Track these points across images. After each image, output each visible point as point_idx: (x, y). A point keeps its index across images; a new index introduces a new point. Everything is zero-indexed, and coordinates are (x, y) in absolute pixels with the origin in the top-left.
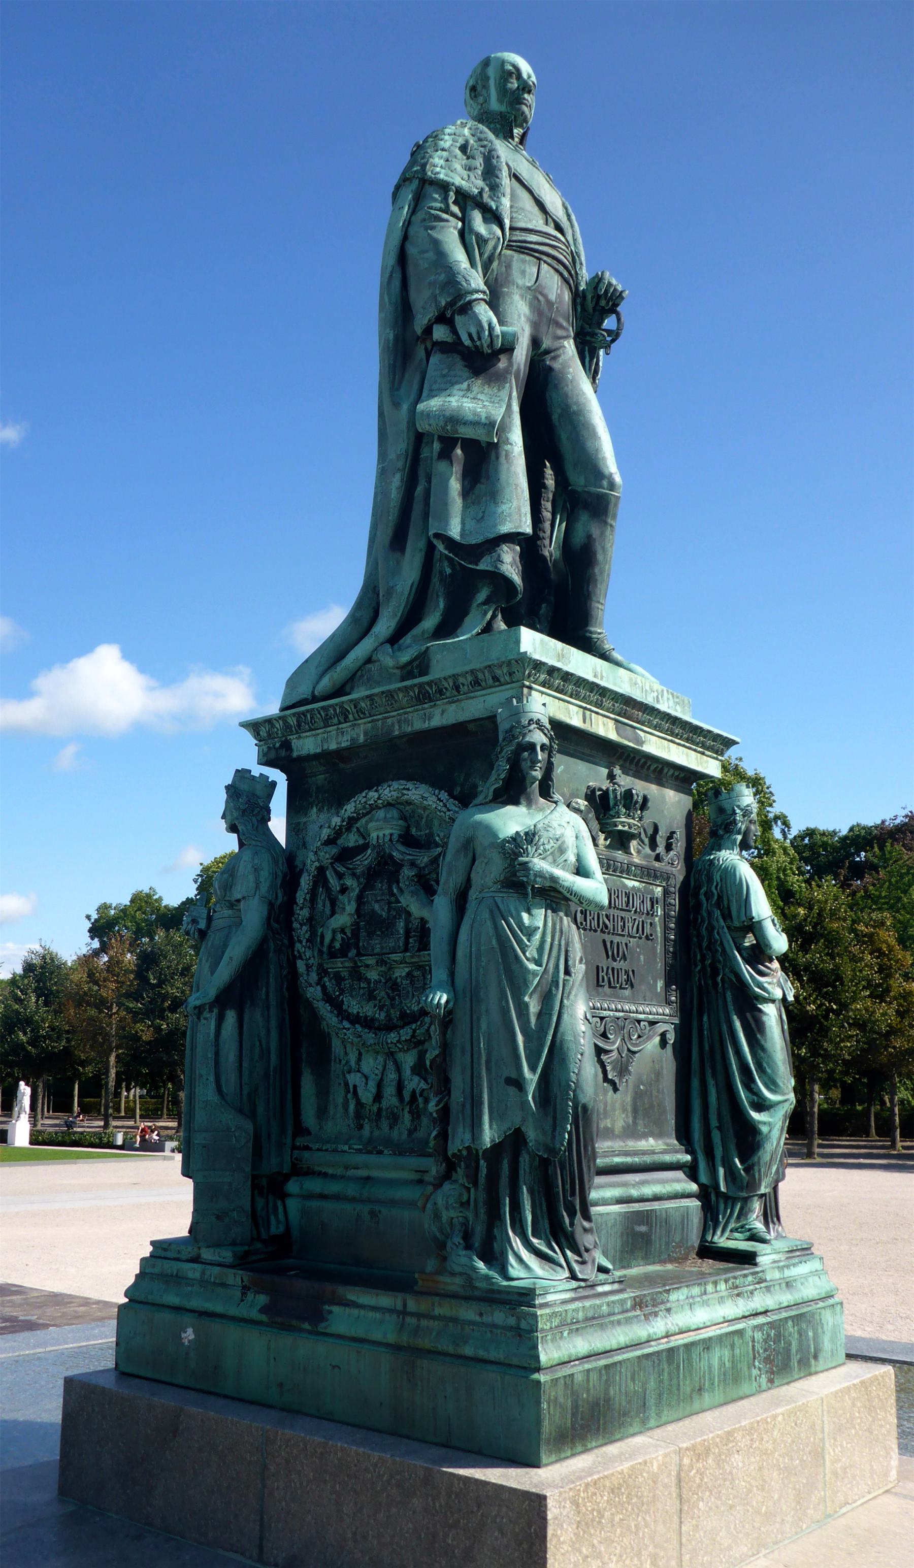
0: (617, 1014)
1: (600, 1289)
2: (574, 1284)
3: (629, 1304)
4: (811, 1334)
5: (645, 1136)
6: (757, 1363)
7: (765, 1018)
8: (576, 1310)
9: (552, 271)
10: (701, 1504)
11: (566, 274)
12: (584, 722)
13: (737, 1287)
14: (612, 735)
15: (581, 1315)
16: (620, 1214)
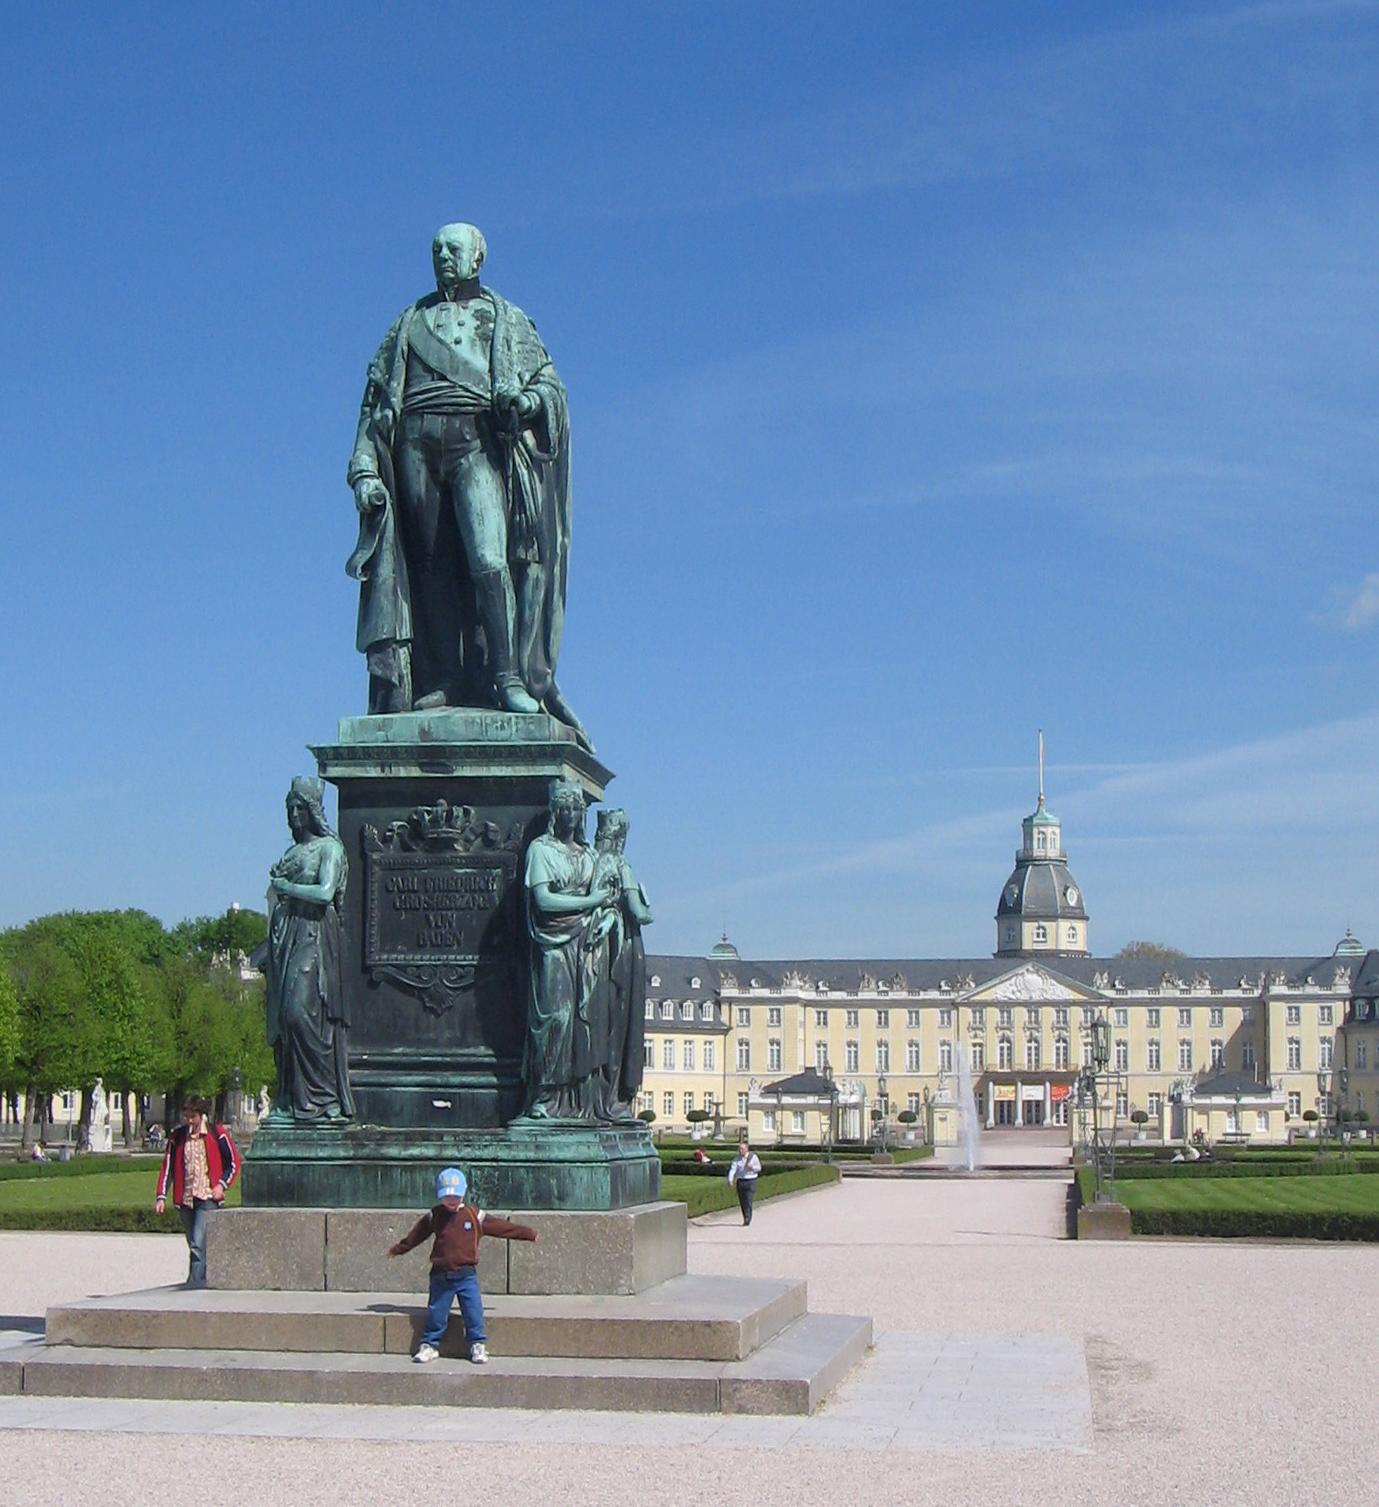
0: (438, 963)
1: (319, 1126)
2: (292, 1121)
3: (340, 1137)
4: (553, 1182)
5: (476, 1045)
6: (474, 1190)
7: (545, 959)
8: (289, 1134)
9: (436, 416)
10: (349, 1248)
11: (450, 409)
12: (383, 771)
13: (469, 1141)
14: (415, 772)
15: (292, 1137)
16: (416, 1092)
